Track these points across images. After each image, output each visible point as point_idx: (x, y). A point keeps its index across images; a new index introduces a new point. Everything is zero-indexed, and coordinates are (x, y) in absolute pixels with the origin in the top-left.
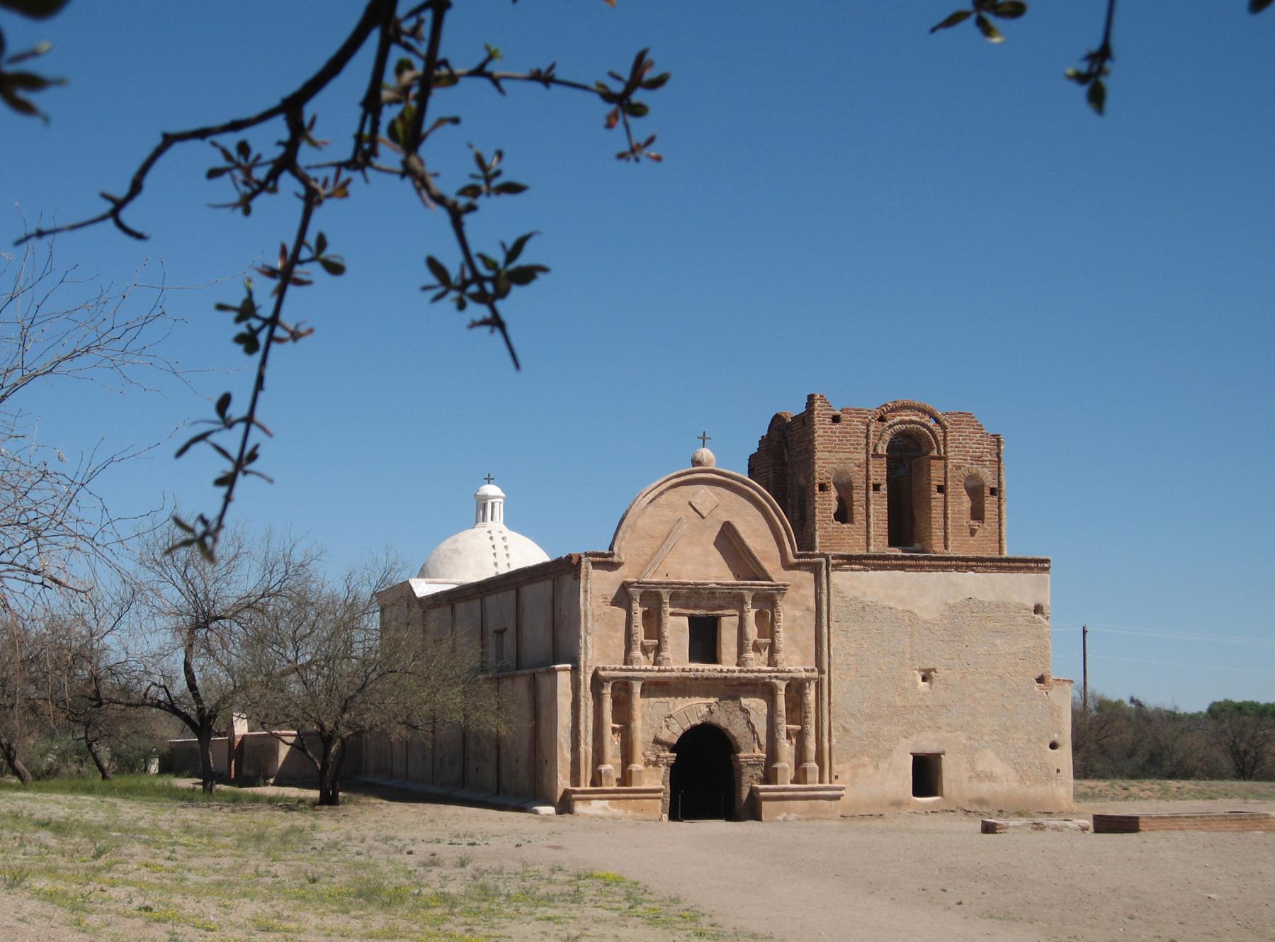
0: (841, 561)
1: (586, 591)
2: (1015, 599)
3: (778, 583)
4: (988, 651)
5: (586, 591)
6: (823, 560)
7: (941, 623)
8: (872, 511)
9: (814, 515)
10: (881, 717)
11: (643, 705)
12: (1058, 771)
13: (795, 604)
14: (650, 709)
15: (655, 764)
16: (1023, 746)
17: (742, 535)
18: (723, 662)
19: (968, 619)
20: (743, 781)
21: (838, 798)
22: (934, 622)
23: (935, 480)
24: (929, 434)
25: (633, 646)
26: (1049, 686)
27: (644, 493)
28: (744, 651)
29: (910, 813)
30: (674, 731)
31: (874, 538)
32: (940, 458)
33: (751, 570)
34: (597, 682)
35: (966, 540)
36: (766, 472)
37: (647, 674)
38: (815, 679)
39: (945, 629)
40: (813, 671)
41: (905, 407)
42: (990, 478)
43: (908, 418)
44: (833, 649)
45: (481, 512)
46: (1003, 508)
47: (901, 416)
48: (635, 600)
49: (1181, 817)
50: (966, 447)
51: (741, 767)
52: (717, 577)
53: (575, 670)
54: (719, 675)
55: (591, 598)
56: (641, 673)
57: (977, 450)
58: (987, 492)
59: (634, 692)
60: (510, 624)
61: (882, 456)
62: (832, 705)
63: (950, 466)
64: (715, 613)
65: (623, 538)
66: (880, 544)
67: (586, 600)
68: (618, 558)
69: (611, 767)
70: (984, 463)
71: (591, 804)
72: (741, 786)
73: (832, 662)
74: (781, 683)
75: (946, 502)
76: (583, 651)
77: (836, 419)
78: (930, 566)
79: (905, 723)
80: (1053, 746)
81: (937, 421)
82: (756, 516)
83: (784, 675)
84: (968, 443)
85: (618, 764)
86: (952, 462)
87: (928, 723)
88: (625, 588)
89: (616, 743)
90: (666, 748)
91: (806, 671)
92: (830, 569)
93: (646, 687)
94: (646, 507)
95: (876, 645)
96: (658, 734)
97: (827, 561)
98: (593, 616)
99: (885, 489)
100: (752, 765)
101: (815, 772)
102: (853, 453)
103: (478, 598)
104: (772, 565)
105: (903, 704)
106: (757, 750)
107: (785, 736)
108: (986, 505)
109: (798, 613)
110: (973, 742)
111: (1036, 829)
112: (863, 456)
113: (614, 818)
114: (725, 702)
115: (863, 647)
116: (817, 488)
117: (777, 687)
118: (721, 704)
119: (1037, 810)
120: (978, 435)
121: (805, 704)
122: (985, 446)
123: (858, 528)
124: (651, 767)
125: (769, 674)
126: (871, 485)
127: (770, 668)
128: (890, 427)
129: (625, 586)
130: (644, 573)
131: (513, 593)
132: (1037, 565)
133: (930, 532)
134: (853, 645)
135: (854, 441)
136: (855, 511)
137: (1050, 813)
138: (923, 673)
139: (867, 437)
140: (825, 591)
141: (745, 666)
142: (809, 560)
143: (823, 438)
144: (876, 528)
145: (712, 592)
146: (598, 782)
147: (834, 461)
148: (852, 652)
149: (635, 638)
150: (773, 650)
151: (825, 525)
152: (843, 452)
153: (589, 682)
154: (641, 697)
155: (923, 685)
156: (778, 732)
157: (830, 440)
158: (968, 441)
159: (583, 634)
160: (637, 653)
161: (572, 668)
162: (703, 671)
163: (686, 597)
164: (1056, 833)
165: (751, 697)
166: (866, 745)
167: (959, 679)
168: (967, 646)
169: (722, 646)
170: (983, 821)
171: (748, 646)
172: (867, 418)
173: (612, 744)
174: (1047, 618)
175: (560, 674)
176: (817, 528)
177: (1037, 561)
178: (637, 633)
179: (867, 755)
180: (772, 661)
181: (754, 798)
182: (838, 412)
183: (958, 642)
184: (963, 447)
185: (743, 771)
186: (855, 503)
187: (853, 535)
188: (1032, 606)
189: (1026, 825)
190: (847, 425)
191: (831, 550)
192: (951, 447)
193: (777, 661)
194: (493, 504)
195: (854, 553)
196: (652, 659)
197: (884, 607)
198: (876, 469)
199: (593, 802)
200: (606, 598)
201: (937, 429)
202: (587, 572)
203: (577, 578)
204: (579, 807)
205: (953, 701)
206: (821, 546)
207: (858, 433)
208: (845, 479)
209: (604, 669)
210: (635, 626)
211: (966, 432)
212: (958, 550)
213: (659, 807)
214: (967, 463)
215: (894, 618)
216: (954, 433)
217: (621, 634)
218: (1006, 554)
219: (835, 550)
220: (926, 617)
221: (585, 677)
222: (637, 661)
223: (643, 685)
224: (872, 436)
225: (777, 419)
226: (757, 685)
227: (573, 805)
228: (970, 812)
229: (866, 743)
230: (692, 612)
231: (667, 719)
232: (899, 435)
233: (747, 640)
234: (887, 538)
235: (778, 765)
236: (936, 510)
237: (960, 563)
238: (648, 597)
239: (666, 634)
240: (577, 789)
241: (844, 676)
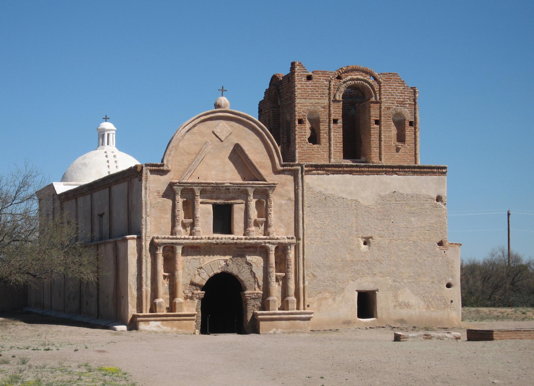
0: (311, 168)
1: (146, 189)
2: (424, 192)
3: (270, 182)
5: (146, 189)
6: (299, 168)
7: (376, 208)
9: (295, 139)
10: (337, 268)
11: (183, 261)
12: (452, 301)
13: (281, 196)
14: (188, 263)
15: (191, 298)
16: (429, 286)
17: (247, 152)
18: (235, 233)
19: (394, 205)
20: (248, 309)
21: (309, 319)
22: (371, 207)
23: (373, 117)
24: (370, 87)
25: (177, 223)
26: (446, 247)
27: (184, 126)
28: (248, 226)
29: (356, 328)
30: (203, 277)
31: (334, 154)
32: (377, 102)
33: (253, 175)
34: (154, 247)
35: (394, 155)
36: (268, 112)
37: (185, 241)
38: (294, 243)
39: (379, 212)
40: (292, 238)
41: (354, 70)
42: (409, 115)
43: (356, 77)
44: (306, 224)
45: (101, 140)
46: (418, 134)
47: (351, 75)
48: (178, 194)
49: (521, 331)
50: (394, 95)
51: (247, 299)
52: (230, 179)
53: (139, 239)
54: (232, 241)
55: (149, 193)
56: (182, 240)
57: (401, 97)
58: (407, 124)
59: (177, 252)
60: (106, 210)
61: (339, 101)
63: (383, 107)
64: (229, 202)
65: (170, 154)
66: (337, 158)
67: (146, 194)
68: (167, 168)
69: (163, 300)
70: (406, 105)
71: (150, 324)
72: (247, 312)
73: (305, 232)
74: (272, 247)
75: (380, 131)
76: (144, 227)
77: (309, 78)
78: (368, 171)
79: (352, 272)
80: (449, 286)
81: (375, 79)
82: (256, 140)
83: (274, 241)
84: (395, 93)
85: (168, 298)
86: (385, 105)
87: (367, 271)
88: (172, 186)
89: (166, 285)
90: (198, 288)
91: (288, 238)
92: (304, 173)
93: (185, 249)
94: (185, 135)
95: (333, 222)
96: (193, 279)
97: (302, 168)
98: (151, 204)
99: (340, 123)
100: (254, 298)
101: (294, 303)
102: (321, 99)
103: (89, 194)
104: (266, 171)
105: (351, 259)
106: (257, 289)
107: (274, 280)
108: (406, 133)
109: (283, 202)
110: (396, 283)
111: (426, 339)
112: (326, 101)
113: (164, 333)
114: (236, 258)
115: (325, 223)
116: (297, 122)
117: (269, 249)
118: (234, 260)
119: (438, 326)
121: (288, 260)
124: (188, 300)
125: (264, 241)
126: (332, 120)
127: (265, 237)
128: (344, 82)
129: (171, 185)
130: (183, 177)
131: (108, 190)
132: (440, 170)
133: (370, 150)
134: (319, 222)
135: (321, 92)
136: (321, 137)
137: (446, 328)
138: (364, 240)
139: (329, 89)
140: (301, 188)
141: (248, 236)
142: (290, 168)
143: (300, 90)
144: (335, 147)
145: (227, 189)
146: (154, 310)
147: (308, 105)
148: (318, 226)
149: (177, 218)
150: (267, 225)
151: (302, 146)
152: (313, 99)
153: (148, 246)
154: (182, 256)
155: (364, 247)
156: (270, 277)
158: (395, 91)
159: (144, 216)
160: (179, 228)
161: (138, 238)
162: (222, 239)
163: (211, 192)
164: (439, 340)
165: (253, 256)
166: (327, 286)
167: (387, 243)
168: (393, 222)
169: (234, 223)
170: (395, 333)
171: (251, 223)
172: (329, 77)
173: (163, 286)
174: (445, 204)
175: (130, 242)
176: (297, 148)
177: (438, 168)
178: (179, 215)
179: (328, 292)
180: (266, 233)
181: (256, 319)
182: (310, 73)
183: (387, 219)
184: (392, 95)
185: (248, 302)
186: (321, 132)
187: (320, 152)
188: (435, 197)
189: (420, 336)
190: (316, 81)
191: (306, 162)
193: (269, 232)
194: (108, 135)
195: (320, 163)
196: (189, 231)
197: (339, 198)
198: (335, 109)
199: (151, 322)
200: (159, 193)
201: (375, 84)
202: (147, 176)
203: (141, 180)
204: (142, 326)
205: (383, 257)
206: (299, 159)
207: (323, 86)
208: (315, 116)
209: (158, 238)
210: (177, 211)
211: (393, 86)
212: (388, 161)
213: (194, 325)
214: (394, 106)
216: (386, 87)
217: (169, 216)
218: (419, 163)
219: (308, 161)
220: (366, 204)
221: (145, 243)
222: (179, 233)
223: (183, 248)
224: (332, 88)
225: (274, 78)
226: (257, 248)
227: (138, 325)
228: (394, 327)
229: (327, 284)
230: (214, 201)
231: (199, 270)
232: (349, 87)
233: (250, 219)
234: (342, 153)
235: (270, 298)
237: (388, 169)
238: (186, 192)
239: (198, 216)
240: (140, 314)
241: (313, 242)
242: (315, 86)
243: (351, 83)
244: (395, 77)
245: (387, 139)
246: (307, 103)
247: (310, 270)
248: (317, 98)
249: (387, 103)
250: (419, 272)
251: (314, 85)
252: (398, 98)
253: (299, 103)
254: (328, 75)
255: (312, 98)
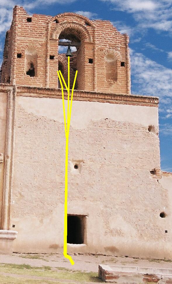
4: (118, 151)
6: (11, 88)
8: (48, 69)
16: (142, 214)
22: (83, 131)
23: (87, 55)
26: (159, 176)
32: (91, 43)
42: (121, 57)
50: (106, 39)
62: (13, 179)
63: (97, 48)
73: (14, 151)
86: (98, 47)
87: (78, 195)
92: (16, 94)
110: (108, 209)
116: (16, 55)
120: (113, 33)
122: (118, 39)
123: (39, 78)
134: (29, 142)
135: (39, 32)
143: (21, 29)
147: (27, 42)
152: (32, 37)
157: (25, 30)
158: (107, 36)
167: (99, 167)
172: (47, 20)
182: (30, 16)
184: (104, 39)
186: (38, 65)
188: (147, 126)
190: (35, 23)
192: (98, 38)
197: (51, 120)
198: (52, 47)
205: (94, 181)
215: (57, 127)
216: (99, 31)
224: (50, 29)
229: (35, 205)
236: (88, 72)
242: (34, 27)
243: (67, 26)
244: (107, 24)
245: (100, 75)
246: (26, 41)
247: (17, 189)
248: (36, 36)
249: (101, 45)
250: (131, 199)
251: (34, 26)
252: (110, 42)
253: (19, 40)
254: (45, 19)
255: (31, 36)
